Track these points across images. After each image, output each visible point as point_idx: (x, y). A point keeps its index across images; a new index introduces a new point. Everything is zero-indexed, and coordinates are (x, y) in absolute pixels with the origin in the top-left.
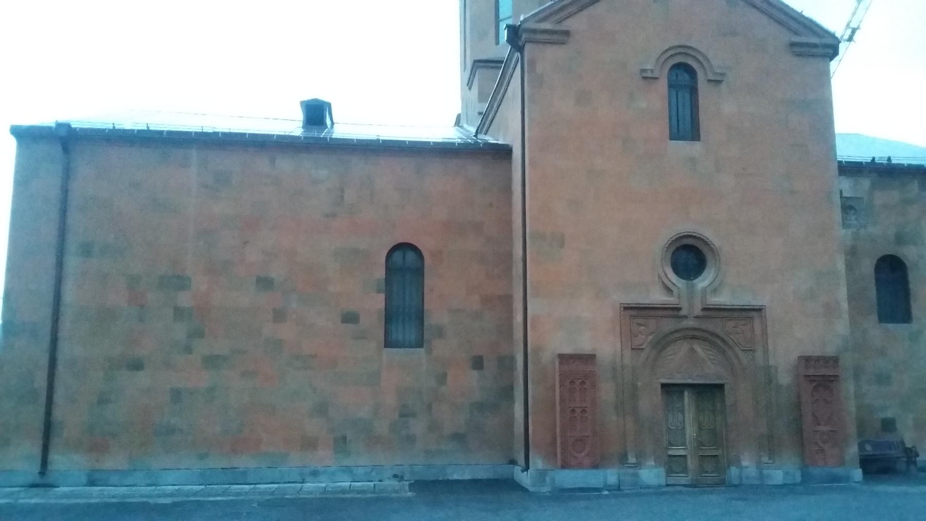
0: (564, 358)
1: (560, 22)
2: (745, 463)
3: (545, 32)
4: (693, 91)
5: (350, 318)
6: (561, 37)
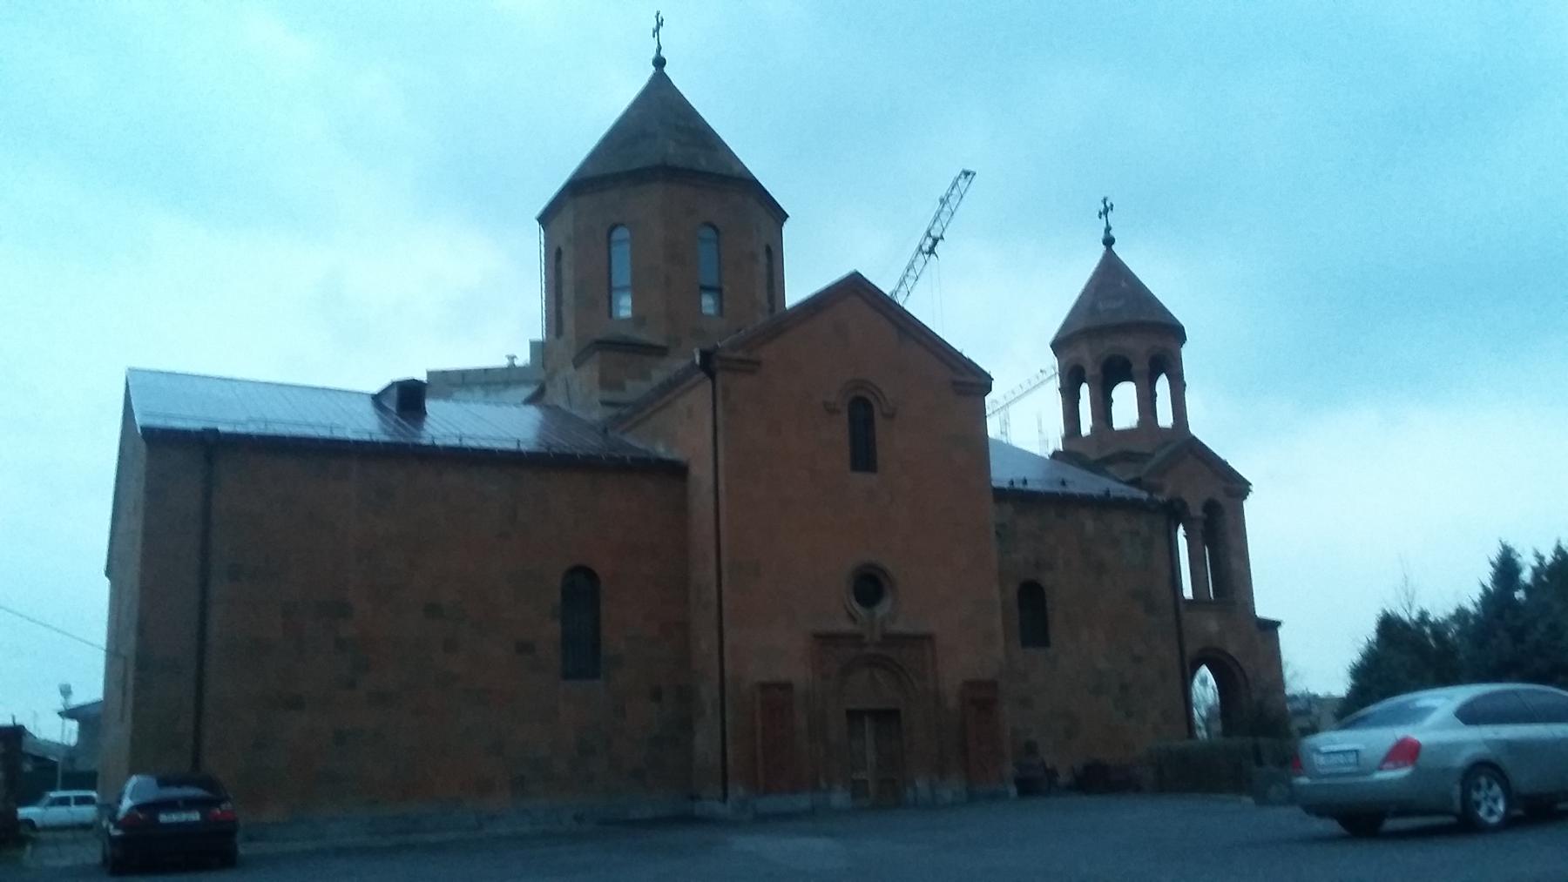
0: (765, 687)
2: (919, 784)
3: (741, 361)
4: (869, 422)
5: (524, 648)
6: (750, 366)
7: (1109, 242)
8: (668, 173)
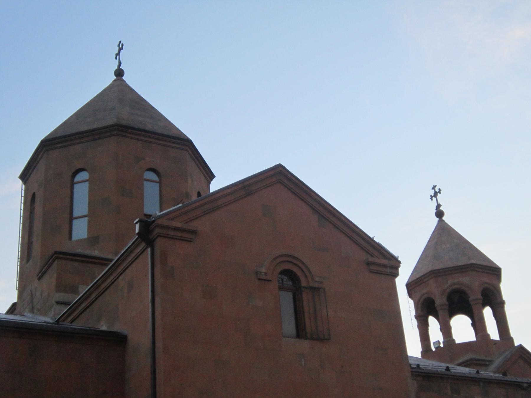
1: (188, 222)
3: (176, 229)
7: (440, 214)
8: (121, 130)
